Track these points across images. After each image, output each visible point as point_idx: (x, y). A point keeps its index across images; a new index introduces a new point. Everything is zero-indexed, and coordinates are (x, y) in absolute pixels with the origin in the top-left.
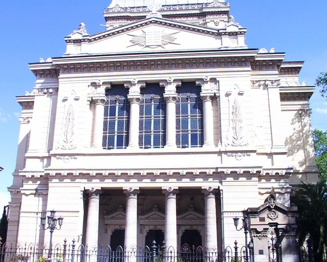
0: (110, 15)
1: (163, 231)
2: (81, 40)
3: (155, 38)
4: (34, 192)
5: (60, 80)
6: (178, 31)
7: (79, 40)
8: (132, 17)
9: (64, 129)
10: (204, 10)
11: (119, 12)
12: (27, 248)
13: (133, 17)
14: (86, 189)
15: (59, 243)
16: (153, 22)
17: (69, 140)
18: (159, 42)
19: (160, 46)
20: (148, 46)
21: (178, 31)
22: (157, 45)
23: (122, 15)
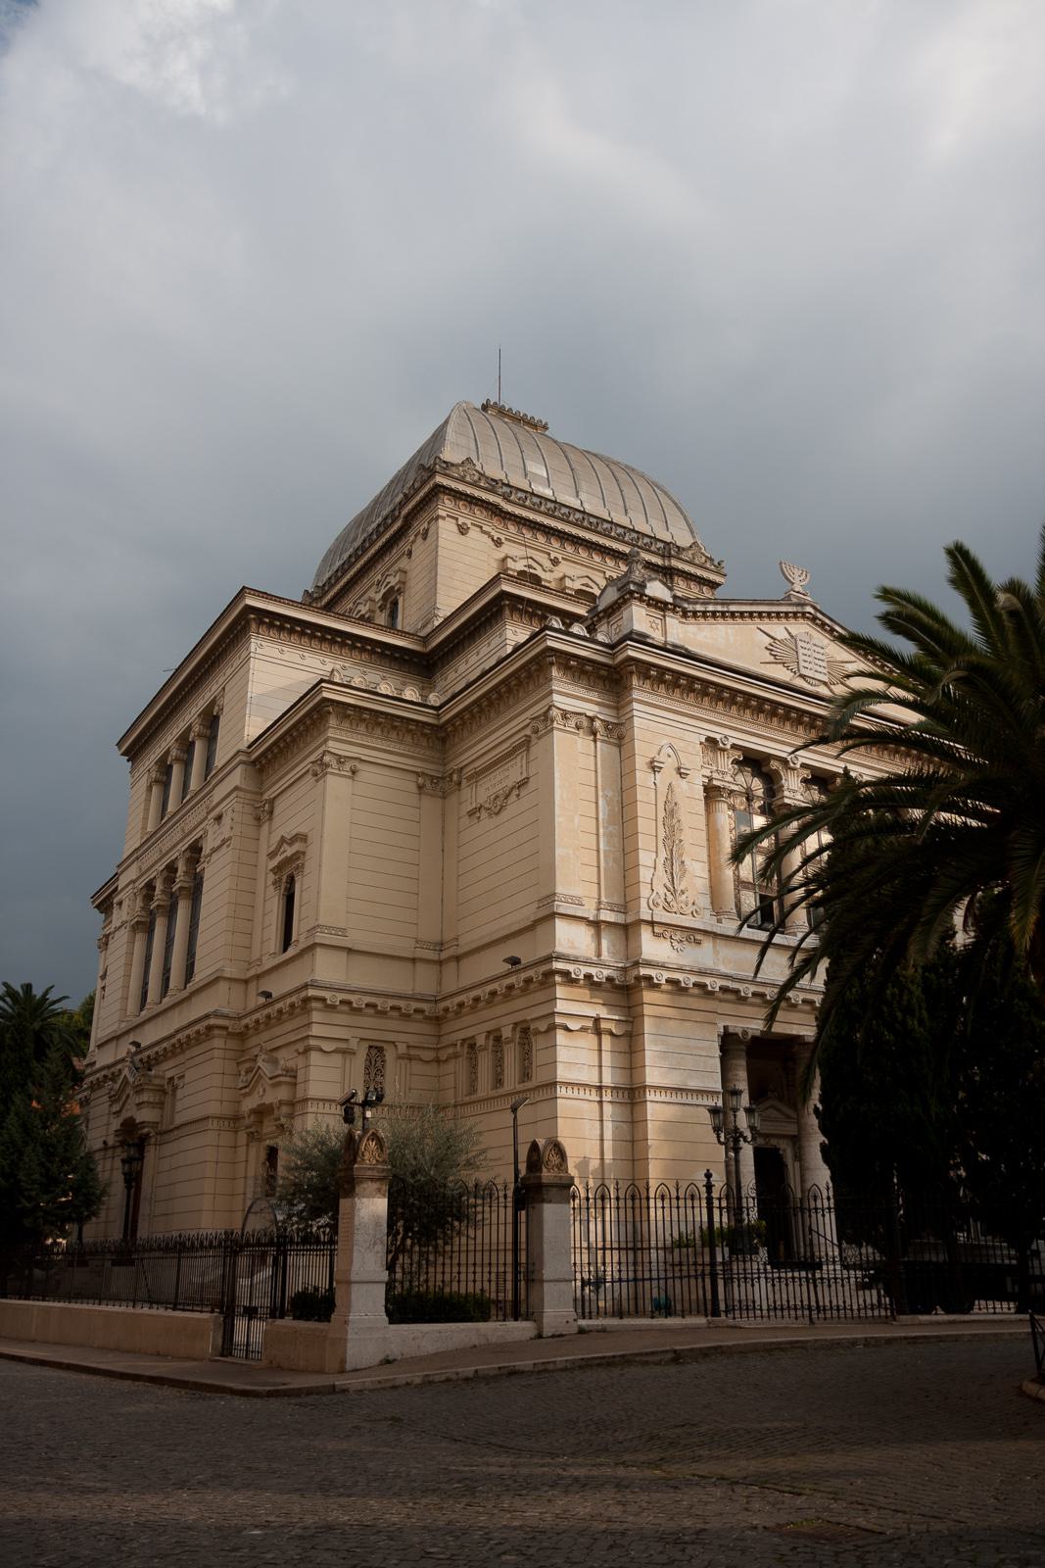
0: (453, 485)
1: (781, 1152)
2: (666, 604)
3: (817, 661)
4: (590, 1024)
5: (635, 705)
6: (853, 659)
7: (661, 602)
8: (503, 512)
9: (663, 854)
10: (675, 563)
11: (474, 484)
12: (681, 1195)
13: (509, 513)
14: (731, 1030)
15: (695, 1182)
16: (808, 618)
17: (679, 888)
18: (825, 674)
19: (825, 683)
20: (803, 676)
21: (853, 659)
22: (819, 680)
23: (484, 496)
